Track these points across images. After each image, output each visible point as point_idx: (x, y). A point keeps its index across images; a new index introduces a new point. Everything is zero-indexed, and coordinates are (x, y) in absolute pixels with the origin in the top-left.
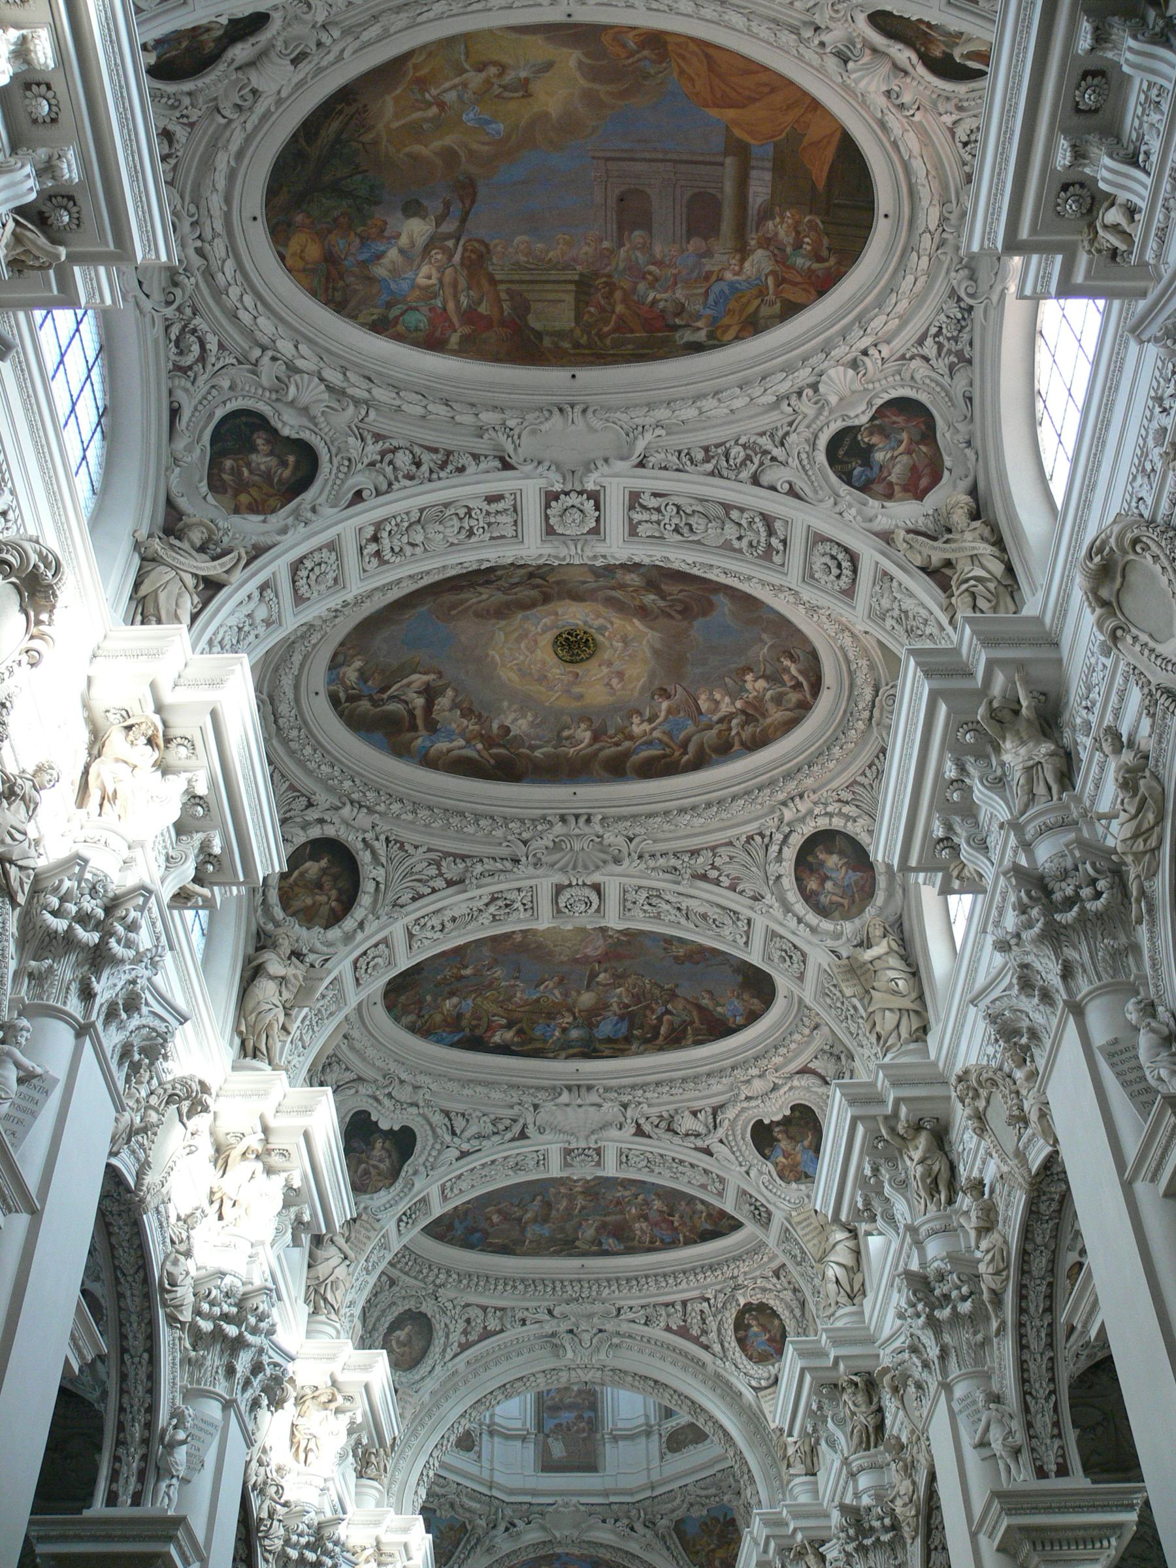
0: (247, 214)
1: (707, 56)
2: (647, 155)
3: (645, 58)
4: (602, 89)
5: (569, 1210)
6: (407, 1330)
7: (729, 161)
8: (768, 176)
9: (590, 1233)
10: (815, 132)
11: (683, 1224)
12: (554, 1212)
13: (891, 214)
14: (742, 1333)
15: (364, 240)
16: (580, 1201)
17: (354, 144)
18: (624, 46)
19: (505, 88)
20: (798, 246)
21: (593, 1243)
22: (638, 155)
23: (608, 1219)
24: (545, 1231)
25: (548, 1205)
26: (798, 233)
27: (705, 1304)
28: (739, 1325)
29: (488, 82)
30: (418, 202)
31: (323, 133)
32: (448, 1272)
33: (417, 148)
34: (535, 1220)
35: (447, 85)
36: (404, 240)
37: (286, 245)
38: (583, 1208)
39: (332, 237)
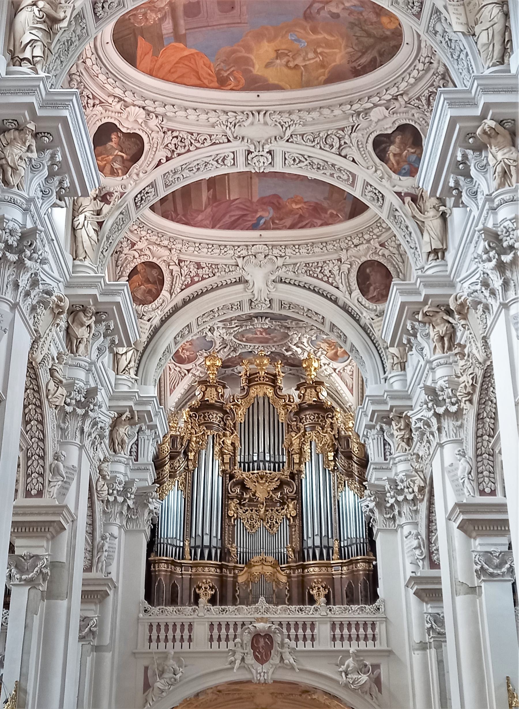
0: (409, 48)
1: (200, 79)
2: (221, 26)
3: (226, 71)
4: (244, 54)
7: (183, 32)
8: (164, 32)
10: (148, 58)
13: (106, 45)
15: (361, 13)
17: (356, 48)
18: (235, 78)
19: (287, 55)
20: (145, 14)
22: (225, 26)
26: (146, 18)
29: (294, 59)
30: (332, 17)
31: (369, 59)
33: (329, 37)
35: (312, 61)
36: (341, 6)
37: (396, 28)
39: (375, 20)
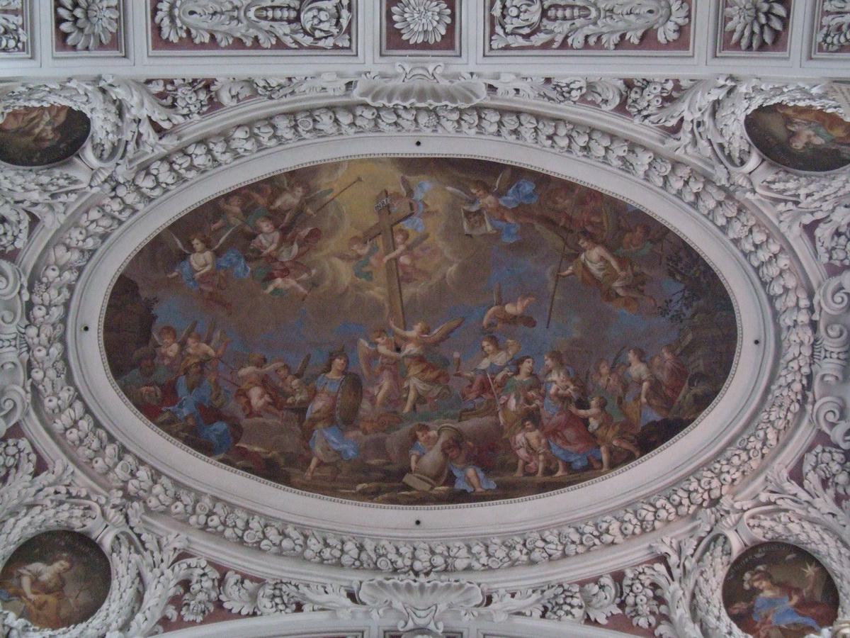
5: (395, 400)
6: (57, 566)
9: (433, 458)
11: (607, 422)
12: (365, 405)
14: (740, 607)
16: (415, 383)
21: (436, 478)
23: (468, 425)
24: (347, 444)
25: (355, 384)
27: (660, 568)
28: (734, 593)
32: (156, 475)
34: (329, 418)
38: (420, 399)
